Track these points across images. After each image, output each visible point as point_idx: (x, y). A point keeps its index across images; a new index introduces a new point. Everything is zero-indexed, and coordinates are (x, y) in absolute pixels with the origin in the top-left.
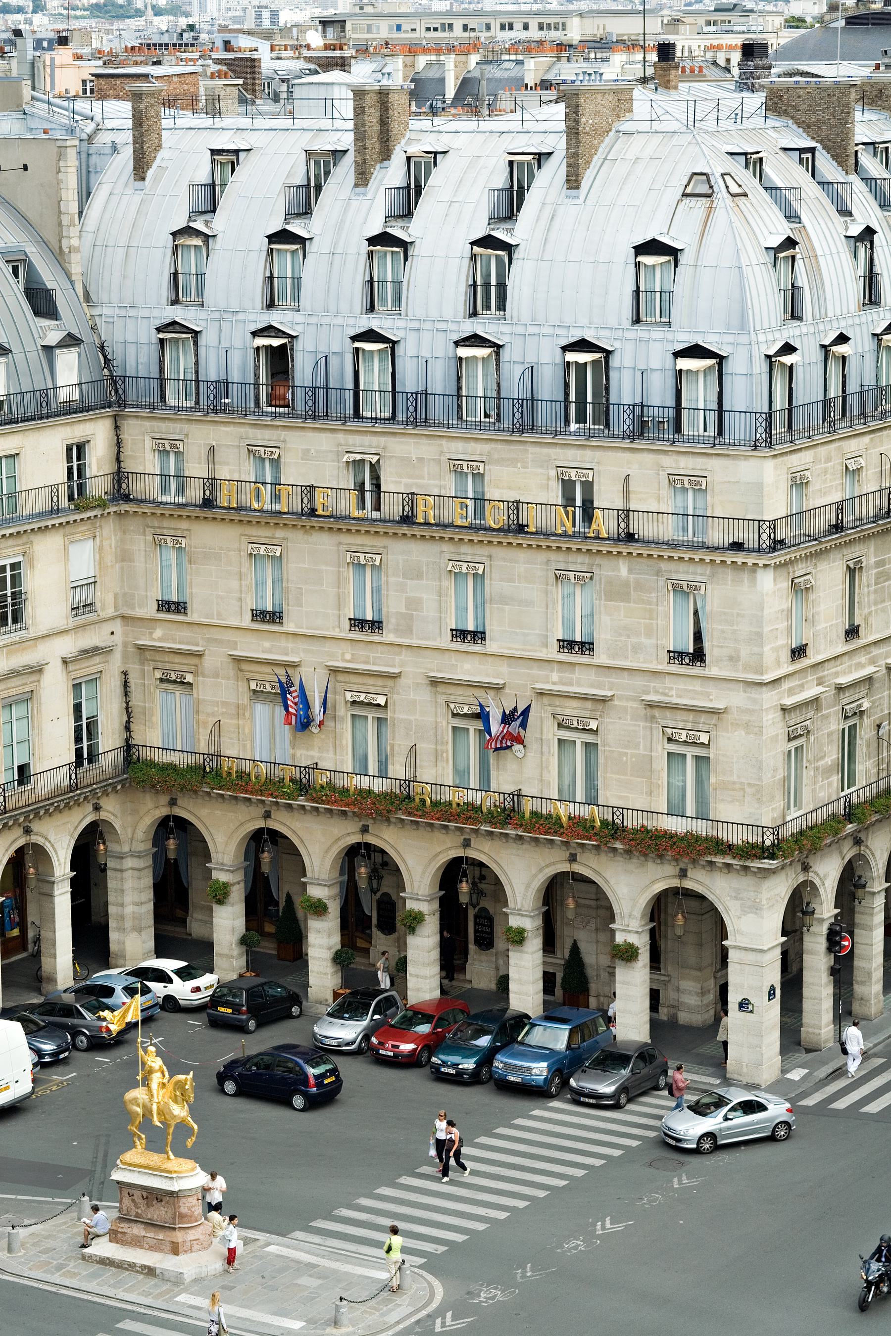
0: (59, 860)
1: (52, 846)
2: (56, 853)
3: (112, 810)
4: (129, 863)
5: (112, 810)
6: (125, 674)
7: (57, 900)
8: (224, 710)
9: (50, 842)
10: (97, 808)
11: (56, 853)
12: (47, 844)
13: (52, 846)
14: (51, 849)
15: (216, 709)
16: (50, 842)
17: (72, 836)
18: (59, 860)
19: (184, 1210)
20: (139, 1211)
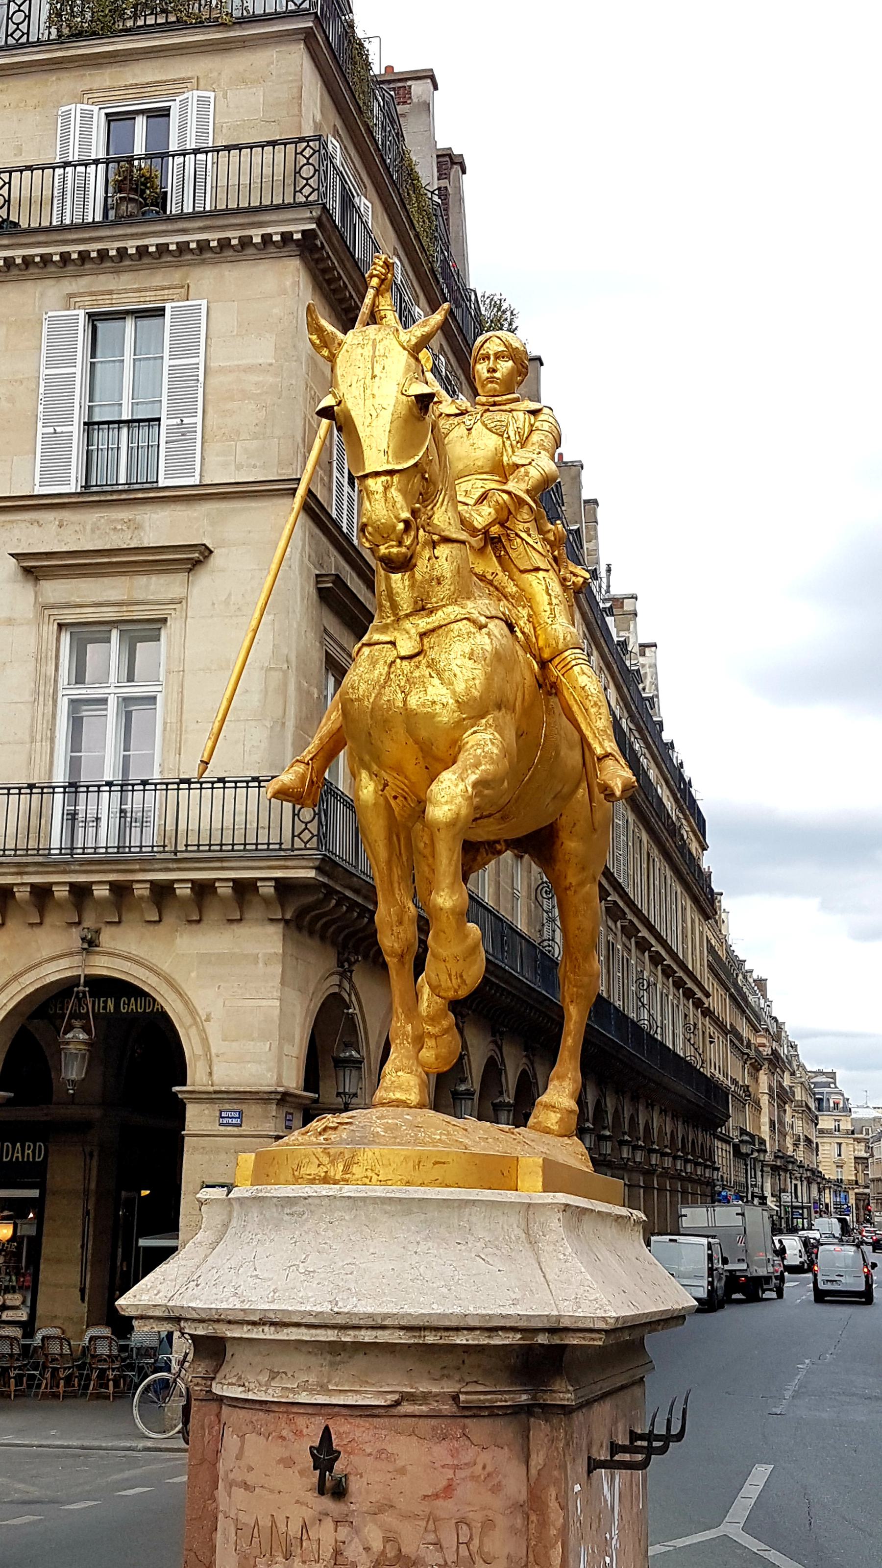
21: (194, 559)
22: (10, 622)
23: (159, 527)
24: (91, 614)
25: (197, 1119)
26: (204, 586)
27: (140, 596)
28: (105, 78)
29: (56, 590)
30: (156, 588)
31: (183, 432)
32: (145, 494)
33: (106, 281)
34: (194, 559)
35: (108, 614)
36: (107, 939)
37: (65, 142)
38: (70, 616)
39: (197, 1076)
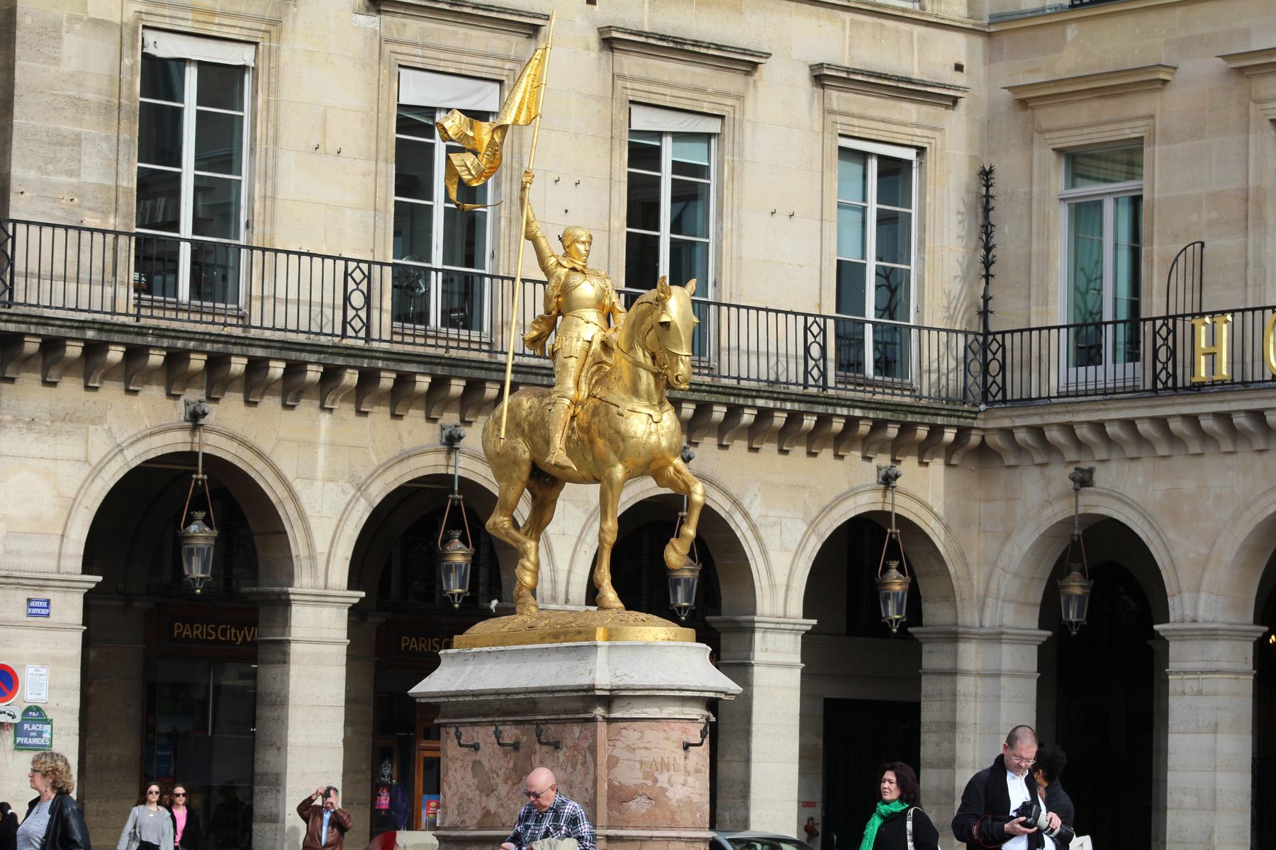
0: (769, 572)
1: (753, 528)
2: (764, 552)
5: (925, 491)
6: (986, 175)
8: (1214, 215)
9: (746, 515)
10: (888, 480)
11: (764, 552)
12: (738, 517)
13: (753, 528)
14: (749, 535)
15: (1194, 217)
16: (746, 515)
17: (813, 525)
18: (769, 572)
19: (628, 775)
20: (492, 804)
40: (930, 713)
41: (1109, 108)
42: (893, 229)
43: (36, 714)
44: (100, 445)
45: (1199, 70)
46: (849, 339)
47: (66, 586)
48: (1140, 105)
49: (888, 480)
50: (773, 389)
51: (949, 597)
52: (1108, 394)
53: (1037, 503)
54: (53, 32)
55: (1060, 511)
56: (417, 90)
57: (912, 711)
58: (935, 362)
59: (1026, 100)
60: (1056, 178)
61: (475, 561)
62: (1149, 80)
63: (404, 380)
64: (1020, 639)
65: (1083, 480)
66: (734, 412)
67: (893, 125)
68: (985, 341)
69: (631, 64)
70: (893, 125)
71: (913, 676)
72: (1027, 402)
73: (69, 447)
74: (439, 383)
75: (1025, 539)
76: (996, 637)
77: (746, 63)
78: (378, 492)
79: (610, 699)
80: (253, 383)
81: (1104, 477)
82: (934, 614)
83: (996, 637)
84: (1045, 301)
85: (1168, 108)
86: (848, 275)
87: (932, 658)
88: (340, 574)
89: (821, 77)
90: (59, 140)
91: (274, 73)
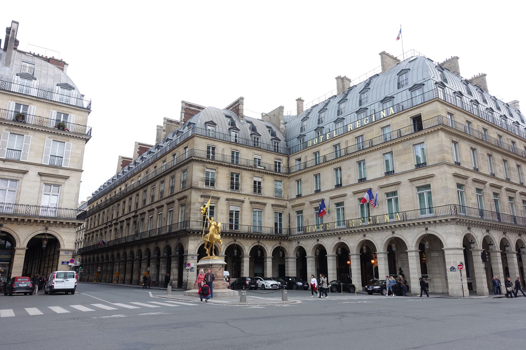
3: (285, 244)
4: (290, 260)
7: (268, 262)
10: (280, 243)
21: (66, 178)
22: (36, 181)
23: (61, 172)
24: (49, 183)
25: (61, 253)
26: (67, 182)
27: (58, 181)
28: (58, 108)
29: (44, 178)
30: (60, 181)
31: (67, 160)
32: (60, 168)
33: (56, 136)
34: (66, 178)
35: (52, 183)
36: (49, 228)
37: (51, 115)
38: (46, 182)
39: (62, 247)
40: (286, 266)
41: (300, 207)
42: (280, 220)
43: (192, 268)
44: (199, 242)
45: (307, 203)
46: (276, 230)
47: (196, 255)
48: (302, 207)
49: (280, 243)
50: (268, 235)
51: (287, 254)
52: (300, 234)
53: (295, 245)
54: (195, 203)
55: (297, 246)
56: (232, 208)
57: (284, 265)
58: (284, 232)
59: (293, 207)
60: (296, 214)
61: (237, 252)
62: (303, 204)
63: (230, 235)
64: (294, 258)
65: (299, 243)
66: (264, 237)
67: (280, 210)
68: (290, 230)
69: (253, 205)
70: (280, 210)
71: (285, 262)
72: (295, 235)
73: (196, 242)
74: (233, 235)
75: (294, 248)
76: (292, 258)
77: (265, 204)
78: (228, 246)
79: (211, 265)
80: (240, 237)
81: (300, 242)
82: (286, 256)
83: (292, 258)
84: (295, 225)
85: (305, 206)
86: (276, 224)
87: (286, 260)
88: (224, 254)
89: (273, 205)
90: (195, 213)
91: (217, 207)
